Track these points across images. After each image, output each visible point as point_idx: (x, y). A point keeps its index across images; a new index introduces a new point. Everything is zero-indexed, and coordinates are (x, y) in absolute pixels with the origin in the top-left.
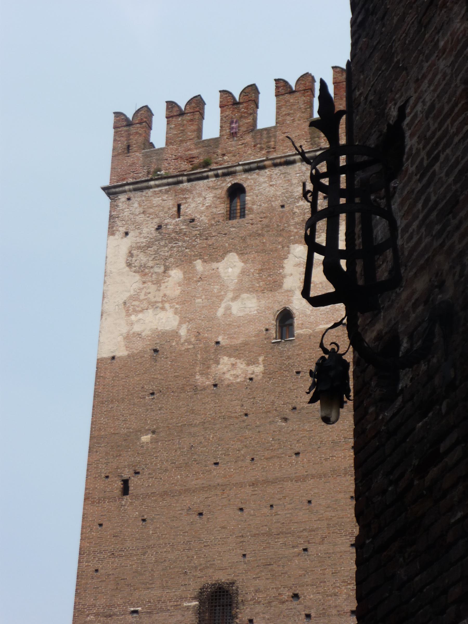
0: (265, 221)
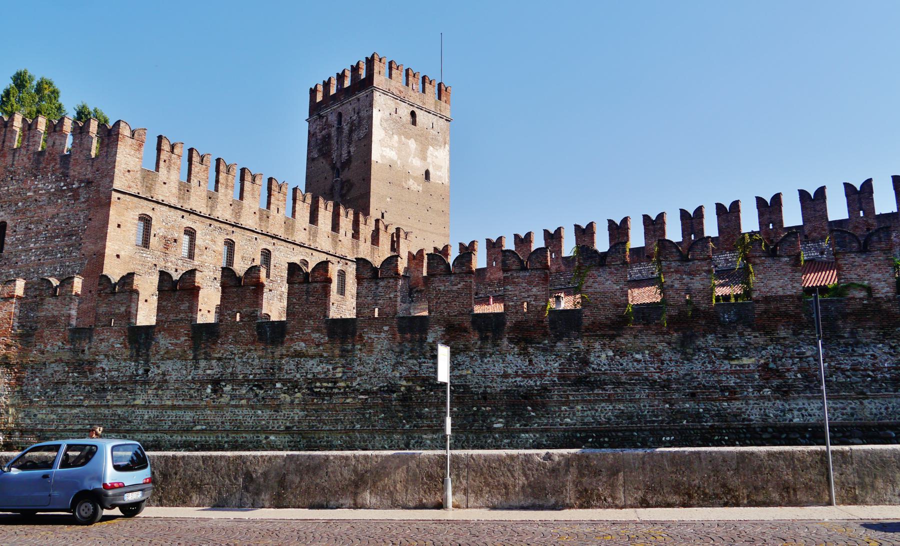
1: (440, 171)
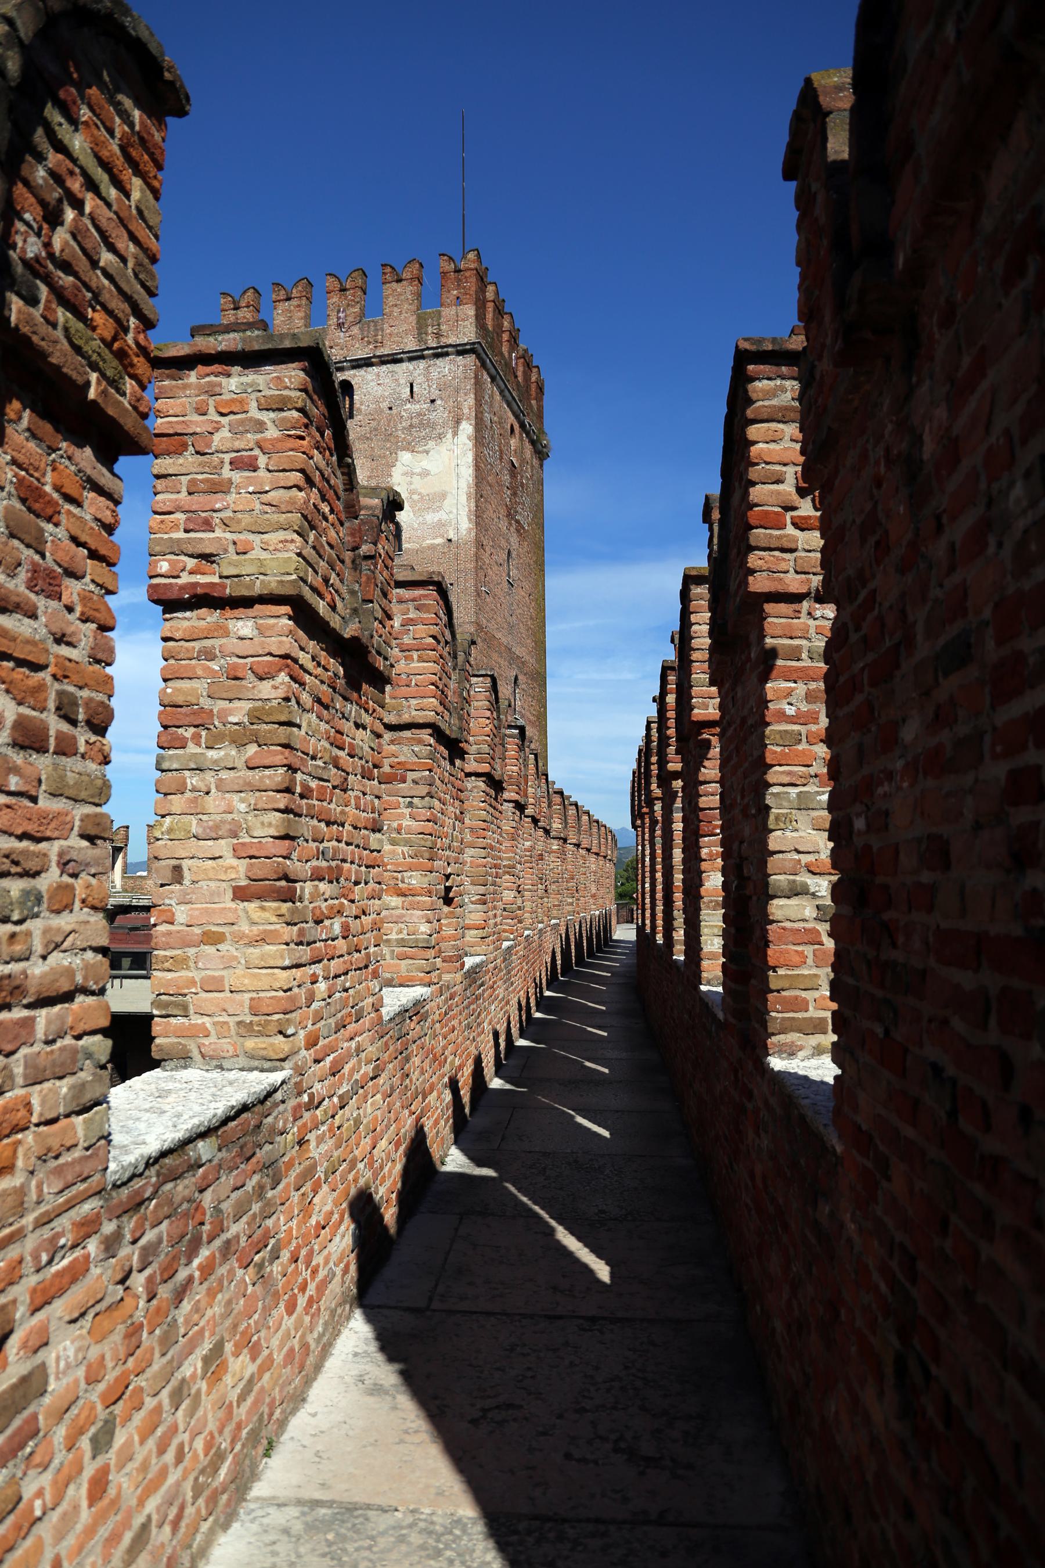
0: (374, 424)
1: (440, 508)
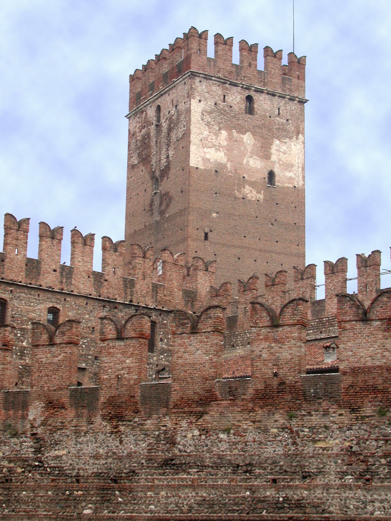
0: (263, 122)
